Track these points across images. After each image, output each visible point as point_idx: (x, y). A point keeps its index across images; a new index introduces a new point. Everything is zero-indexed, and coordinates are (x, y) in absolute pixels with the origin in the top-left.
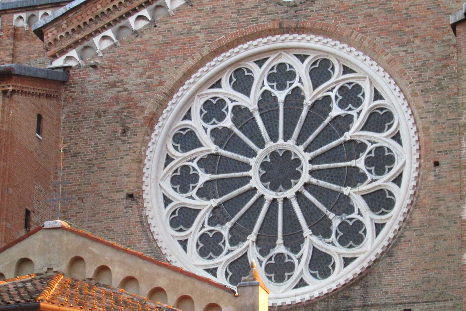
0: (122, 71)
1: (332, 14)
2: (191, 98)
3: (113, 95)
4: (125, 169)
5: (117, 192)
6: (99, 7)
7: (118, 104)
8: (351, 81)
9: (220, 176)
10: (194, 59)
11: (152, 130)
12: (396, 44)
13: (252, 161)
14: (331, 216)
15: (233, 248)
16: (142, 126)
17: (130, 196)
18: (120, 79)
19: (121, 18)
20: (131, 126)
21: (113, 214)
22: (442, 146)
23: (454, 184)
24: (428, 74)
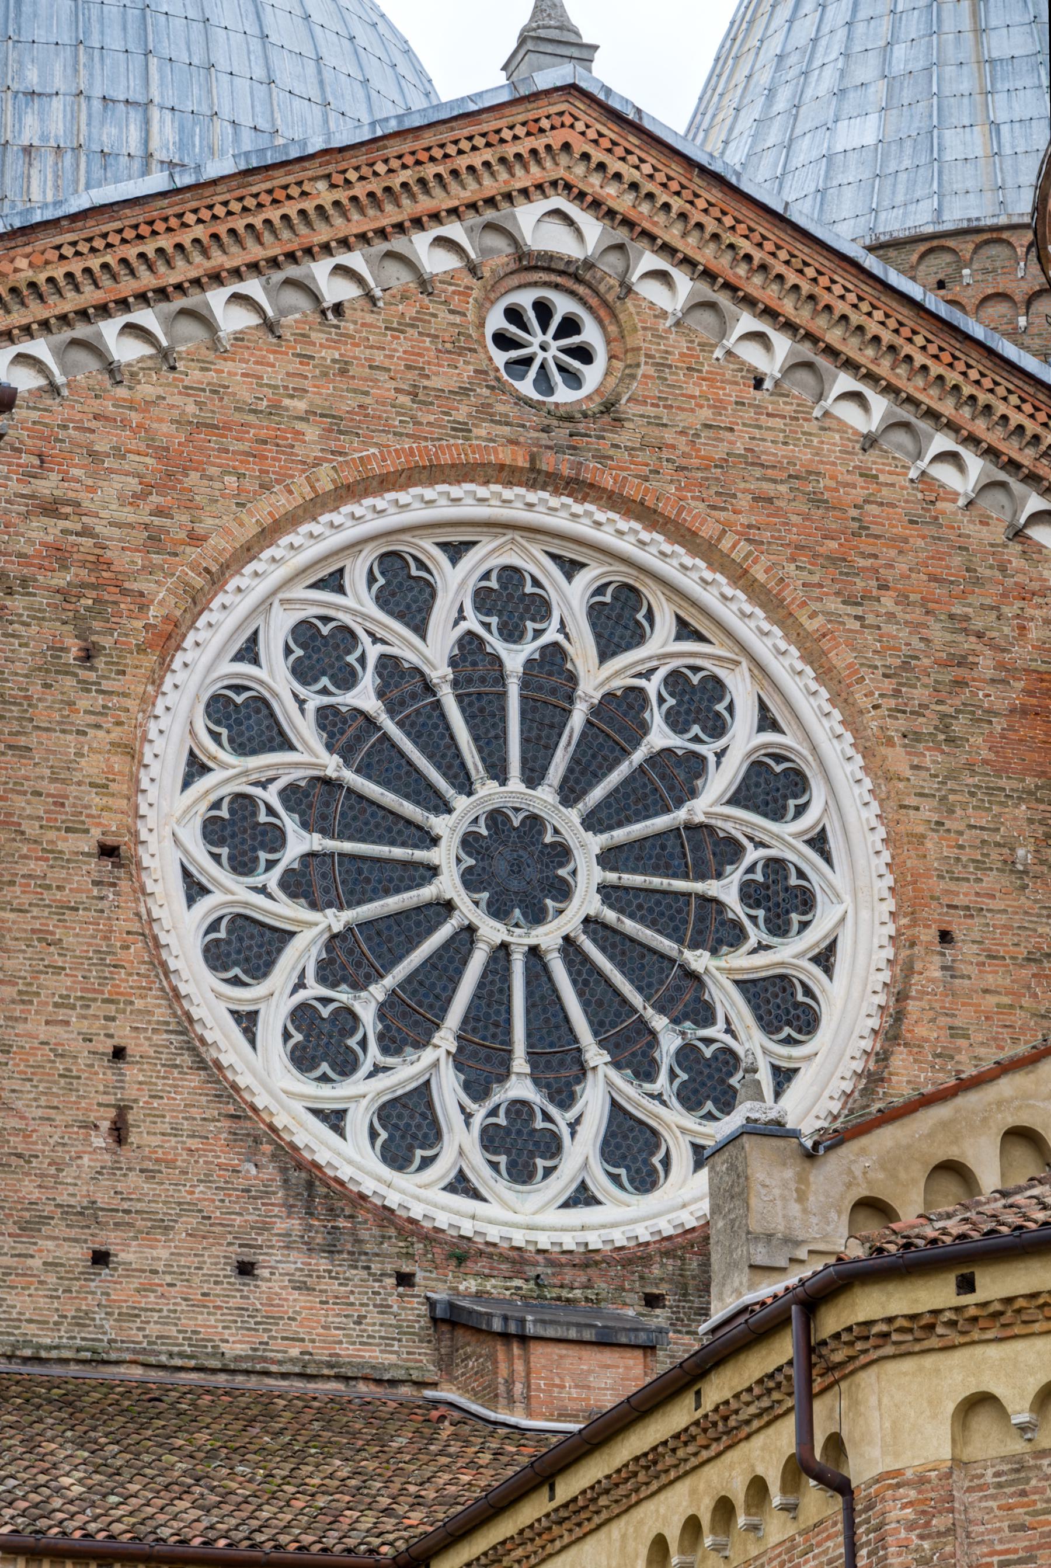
0: (75, 472)
1: (667, 469)
2: (265, 605)
3: (50, 539)
4: (91, 766)
5: (68, 830)
6: (22, 263)
7: (64, 567)
8: (699, 662)
9: (348, 847)
10: (291, 492)
11: (165, 665)
12: (838, 594)
13: (439, 824)
14: (659, 1022)
15: (390, 1061)
16: (141, 649)
17: (108, 851)
18: (71, 495)
19: (83, 314)
20: (107, 642)
21: (59, 896)
22: (957, 894)
23: (992, 1000)
24: (920, 694)
